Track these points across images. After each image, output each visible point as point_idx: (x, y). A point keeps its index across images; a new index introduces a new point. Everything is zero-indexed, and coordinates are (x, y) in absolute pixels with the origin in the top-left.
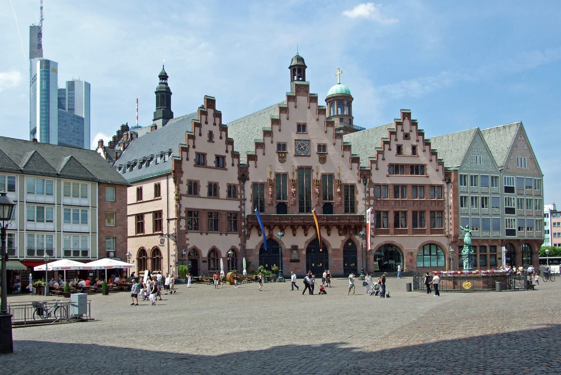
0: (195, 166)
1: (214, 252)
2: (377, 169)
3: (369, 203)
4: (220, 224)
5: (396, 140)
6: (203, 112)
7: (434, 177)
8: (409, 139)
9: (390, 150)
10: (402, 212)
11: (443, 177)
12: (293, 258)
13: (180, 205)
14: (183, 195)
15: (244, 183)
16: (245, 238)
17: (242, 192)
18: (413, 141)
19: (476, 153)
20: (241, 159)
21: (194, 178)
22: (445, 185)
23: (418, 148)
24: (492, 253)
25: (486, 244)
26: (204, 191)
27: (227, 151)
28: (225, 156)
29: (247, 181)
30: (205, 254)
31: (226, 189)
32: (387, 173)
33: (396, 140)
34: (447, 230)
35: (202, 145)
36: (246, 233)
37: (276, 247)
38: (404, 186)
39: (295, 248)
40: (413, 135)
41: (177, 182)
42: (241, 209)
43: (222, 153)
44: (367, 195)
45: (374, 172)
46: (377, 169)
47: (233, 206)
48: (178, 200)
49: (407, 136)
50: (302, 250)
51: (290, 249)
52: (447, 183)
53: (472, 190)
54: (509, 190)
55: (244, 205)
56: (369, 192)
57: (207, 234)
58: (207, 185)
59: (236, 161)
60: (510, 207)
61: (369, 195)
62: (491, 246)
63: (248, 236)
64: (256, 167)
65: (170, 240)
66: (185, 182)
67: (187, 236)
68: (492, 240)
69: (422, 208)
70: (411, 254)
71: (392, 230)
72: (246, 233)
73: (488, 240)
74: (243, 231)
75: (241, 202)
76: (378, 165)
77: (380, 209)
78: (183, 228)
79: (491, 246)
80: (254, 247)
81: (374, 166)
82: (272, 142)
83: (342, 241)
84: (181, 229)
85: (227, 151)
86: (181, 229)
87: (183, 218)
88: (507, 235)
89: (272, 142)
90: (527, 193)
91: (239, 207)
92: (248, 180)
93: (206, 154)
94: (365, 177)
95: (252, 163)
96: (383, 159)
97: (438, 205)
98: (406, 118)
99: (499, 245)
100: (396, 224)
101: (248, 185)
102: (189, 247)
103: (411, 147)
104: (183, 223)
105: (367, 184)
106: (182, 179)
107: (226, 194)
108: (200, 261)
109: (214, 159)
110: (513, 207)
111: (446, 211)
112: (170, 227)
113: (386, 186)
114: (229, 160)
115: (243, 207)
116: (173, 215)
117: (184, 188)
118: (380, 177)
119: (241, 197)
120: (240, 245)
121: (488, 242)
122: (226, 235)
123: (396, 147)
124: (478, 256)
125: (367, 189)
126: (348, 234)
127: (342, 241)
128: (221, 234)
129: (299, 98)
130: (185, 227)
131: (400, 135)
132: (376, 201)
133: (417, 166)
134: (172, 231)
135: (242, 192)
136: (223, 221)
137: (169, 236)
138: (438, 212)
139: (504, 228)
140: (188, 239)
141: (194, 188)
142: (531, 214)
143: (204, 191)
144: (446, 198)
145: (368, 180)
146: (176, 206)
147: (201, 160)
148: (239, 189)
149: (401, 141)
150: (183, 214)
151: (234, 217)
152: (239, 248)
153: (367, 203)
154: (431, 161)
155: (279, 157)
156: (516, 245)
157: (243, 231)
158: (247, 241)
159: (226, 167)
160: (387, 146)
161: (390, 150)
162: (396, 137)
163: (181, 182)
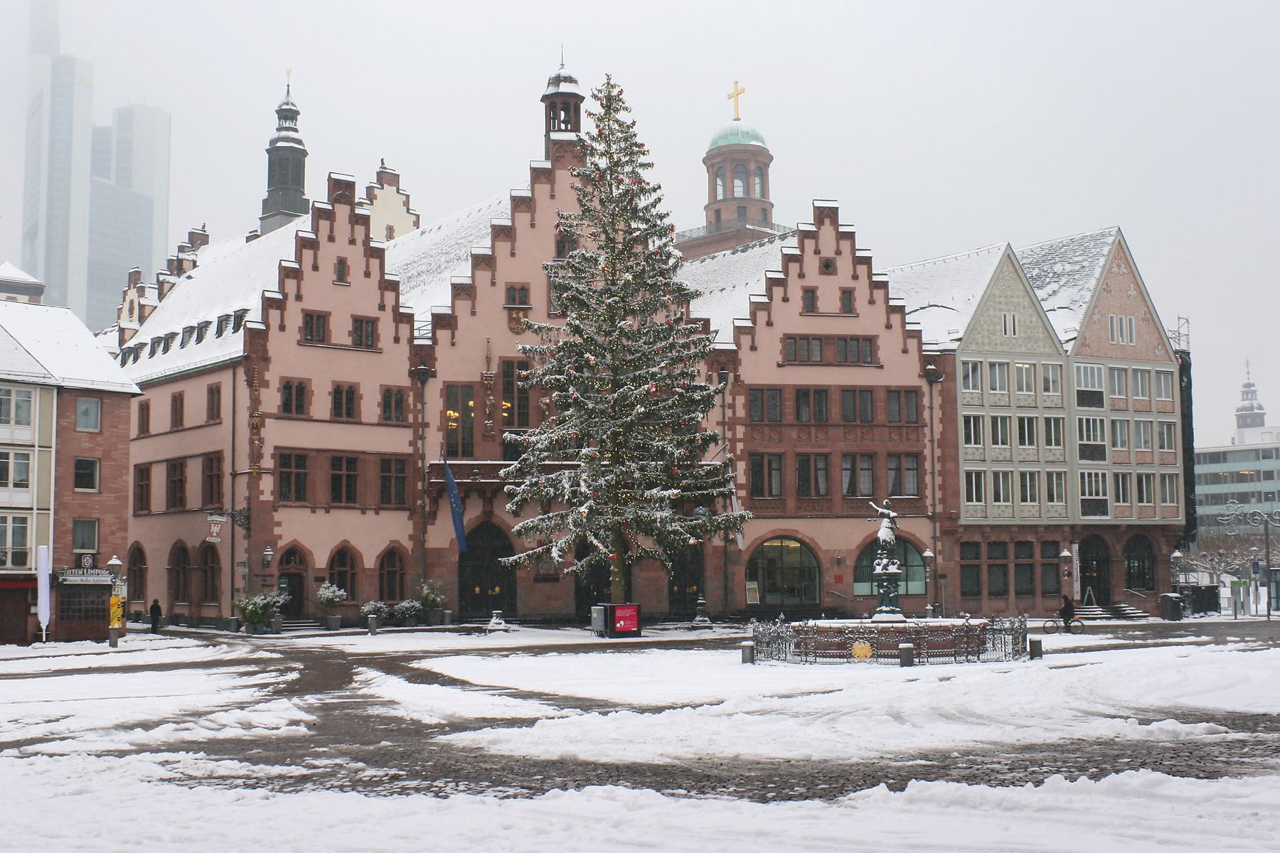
0: (299, 343)
2: (753, 348)
3: (734, 434)
4: (360, 489)
5: (802, 275)
7: (898, 370)
9: (785, 300)
11: (916, 368)
13: (261, 440)
14: (270, 416)
15: (424, 383)
16: (424, 520)
17: (419, 406)
18: (843, 278)
19: (1003, 307)
20: (416, 325)
21: (297, 373)
22: (926, 388)
23: (857, 294)
24: (1046, 561)
25: (1031, 538)
26: (321, 404)
27: (382, 307)
30: (321, 560)
31: (378, 398)
32: (780, 359)
33: (802, 275)
34: (929, 502)
35: (319, 292)
36: (427, 509)
38: (821, 393)
41: (256, 382)
42: (416, 449)
43: (370, 311)
44: (729, 413)
45: (745, 354)
46: (753, 348)
47: (395, 441)
48: (256, 428)
49: (828, 267)
52: (931, 383)
53: (993, 400)
54: (1090, 398)
55: (422, 438)
56: (732, 406)
57: (327, 511)
58: (330, 388)
60: (1092, 442)
61: (734, 413)
62: (1044, 543)
63: (432, 516)
64: (453, 344)
65: (236, 527)
66: (275, 384)
67: (278, 516)
68: (1047, 527)
69: (868, 446)
70: (839, 562)
71: (791, 503)
72: (427, 509)
73: (1036, 526)
74: (419, 502)
75: (416, 432)
77: (762, 450)
78: (267, 496)
79: (1044, 543)
81: (746, 340)
82: (493, 284)
84: (262, 498)
86: (262, 498)
87: (267, 471)
88: (1084, 514)
89: (493, 284)
90: (1138, 407)
92: (434, 375)
93: (329, 314)
95: (443, 335)
96: (769, 324)
97: (908, 439)
98: (827, 221)
99: (1065, 540)
100: (804, 487)
101: (433, 391)
102: (281, 544)
103: (838, 294)
104: (267, 484)
106: (268, 376)
107: (378, 411)
108: (310, 576)
109: (349, 326)
110: (1099, 442)
111: (927, 452)
112: (237, 493)
113: (777, 390)
114: (386, 327)
115: (419, 442)
116: (244, 465)
117: (271, 399)
118: (762, 368)
119: (416, 418)
120: (411, 537)
121: (1037, 533)
122: (377, 513)
123: (800, 293)
124: (1012, 567)
125: (729, 399)
128: (363, 513)
129: (558, 173)
130: (272, 493)
131: (811, 264)
133: (856, 338)
134: (241, 505)
135: (419, 406)
136: (370, 479)
137: (233, 516)
138: (908, 455)
139: (1075, 496)
140: (279, 524)
141: (295, 399)
142: (1148, 459)
143: (321, 404)
144: (928, 421)
145: (731, 375)
146: (251, 442)
147: (315, 328)
148: (411, 400)
149: (813, 277)
150: (268, 462)
152: (408, 545)
153: (729, 435)
154: (889, 326)
155: (511, 319)
156: (1109, 538)
157: (419, 502)
158: (429, 527)
159: (380, 345)
161: (785, 300)
163: (266, 384)
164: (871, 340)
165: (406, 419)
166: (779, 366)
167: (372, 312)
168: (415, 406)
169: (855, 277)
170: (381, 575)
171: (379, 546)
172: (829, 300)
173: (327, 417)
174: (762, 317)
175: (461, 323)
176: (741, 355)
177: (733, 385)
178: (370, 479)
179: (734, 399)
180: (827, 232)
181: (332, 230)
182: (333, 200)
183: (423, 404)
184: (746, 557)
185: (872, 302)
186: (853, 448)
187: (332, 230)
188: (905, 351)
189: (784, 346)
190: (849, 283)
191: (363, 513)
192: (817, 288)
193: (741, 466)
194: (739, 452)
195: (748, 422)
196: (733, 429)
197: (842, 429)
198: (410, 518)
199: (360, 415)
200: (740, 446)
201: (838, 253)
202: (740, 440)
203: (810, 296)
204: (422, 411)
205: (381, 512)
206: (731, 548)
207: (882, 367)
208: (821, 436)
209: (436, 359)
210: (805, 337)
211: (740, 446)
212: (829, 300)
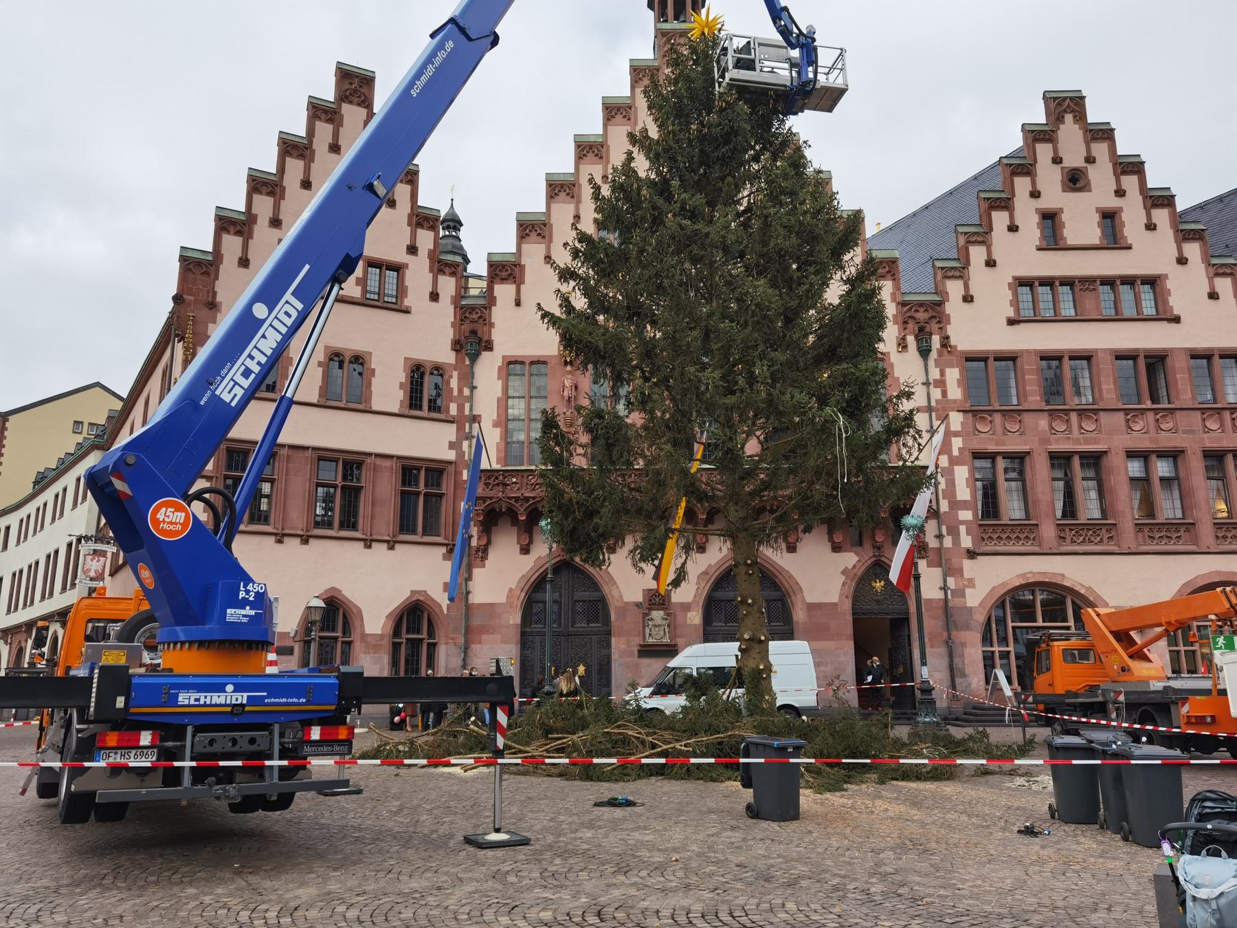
1: (334, 615)
2: (968, 299)
5: (1035, 194)
6: (318, 110)
8: (1086, 188)
9: (1013, 228)
10: (1084, 456)
12: (651, 641)
15: (474, 358)
16: (468, 558)
17: (466, 392)
23: (1125, 216)
27: (412, 250)
28: (405, 266)
29: (485, 354)
31: (402, 376)
33: (1035, 194)
37: (586, 595)
39: (656, 600)
40: (1101, 176)
42: (460, 454)
44: (936, 394)
45: (954, 307)
46: (968, 299)
47: (429, 441)
49: (1075, 180)
50: (686, 607)
51: (638, 605)
56: (941, 383)
59: (447, 285)
61: (944, 394)
63: (484, 551)
64: (518, 304)
69: (1167, 441)
72: (474, 542)
75: (460, 429)
76: (971, 283)
77: (992, 448)
80: (500, 598)
83: (845, 572)
85: (412, 250)
91: (452, 446)
92: (489, 347)
94: (921, 330)
95: (504, 292)
96: (991, 263)
98: (1069, 118)
103: (1097, 218)
105: (934, 355)
113: (1011, 358)
119: (461, 408)
120: (446, 587)
123: (1036, 218)
125: (935, 374)
126: (867, 544)
127: (845, 572)
131: (1049, 177)
132: (974, 413)
133: (1129, 281)
135: (466, 392)
136: (382, 493)
145: (936, 340)
151: (419, 476)
152: (442, 599)
154: (1182, 261)
158: (477, 572)
159: (407, 302)
160: (1000, 219)
161: (1013, 228)
162: (1034, 183)
164: (1152, 281)
165: (448, 410)
166: (1011, 322)
167: (400, 256)
168: (460, 391)
169: (1120, 193)
170: (396, 647)
171: (397, 598)
172: (1081, 224)
173: (314, 399)
174: (977, 254)
175: (528, 276)
176: (949, 308)
177: (940, 354)
178: (382, 493)
179: (942, 373)
180: (1070, 132)
181: (336, 135)
182: (344, 96)
183: (473, 388)
184: (980, 618)
185: (1151, 227)
186: (1145, 444)
187: (336, 135)
188: (1213, 296)
189: (1015, 294)
190: (1112, 202)
191: (368, 544)
192: (1061, 209)
193: (962, 473)
194: (956, 453)
195: (967, 406)
196: (945, 419)
197: (1121, 414)
198: (445, 557)
199: (368, 399)
200: (957, 443)
201: (1090, 160)
202: (956, 434)
203: (1050, 218)
204: (470, 399)
205: (397, 546)
206: (954, 602)
207: (1177, 320)
208: (1089, 426)
209: (492, 325)
210: (1048, 282)
211: (957, 443)
212: (1081, 224)
